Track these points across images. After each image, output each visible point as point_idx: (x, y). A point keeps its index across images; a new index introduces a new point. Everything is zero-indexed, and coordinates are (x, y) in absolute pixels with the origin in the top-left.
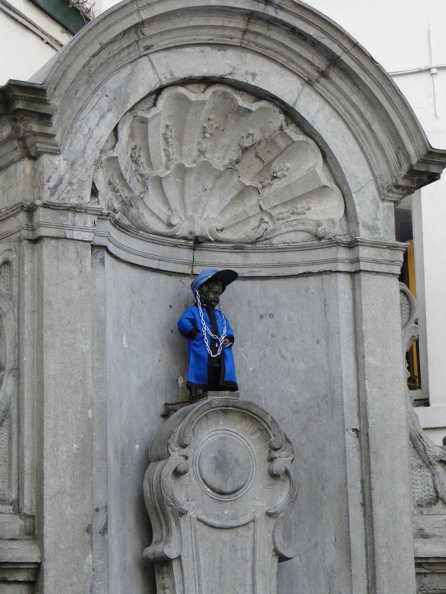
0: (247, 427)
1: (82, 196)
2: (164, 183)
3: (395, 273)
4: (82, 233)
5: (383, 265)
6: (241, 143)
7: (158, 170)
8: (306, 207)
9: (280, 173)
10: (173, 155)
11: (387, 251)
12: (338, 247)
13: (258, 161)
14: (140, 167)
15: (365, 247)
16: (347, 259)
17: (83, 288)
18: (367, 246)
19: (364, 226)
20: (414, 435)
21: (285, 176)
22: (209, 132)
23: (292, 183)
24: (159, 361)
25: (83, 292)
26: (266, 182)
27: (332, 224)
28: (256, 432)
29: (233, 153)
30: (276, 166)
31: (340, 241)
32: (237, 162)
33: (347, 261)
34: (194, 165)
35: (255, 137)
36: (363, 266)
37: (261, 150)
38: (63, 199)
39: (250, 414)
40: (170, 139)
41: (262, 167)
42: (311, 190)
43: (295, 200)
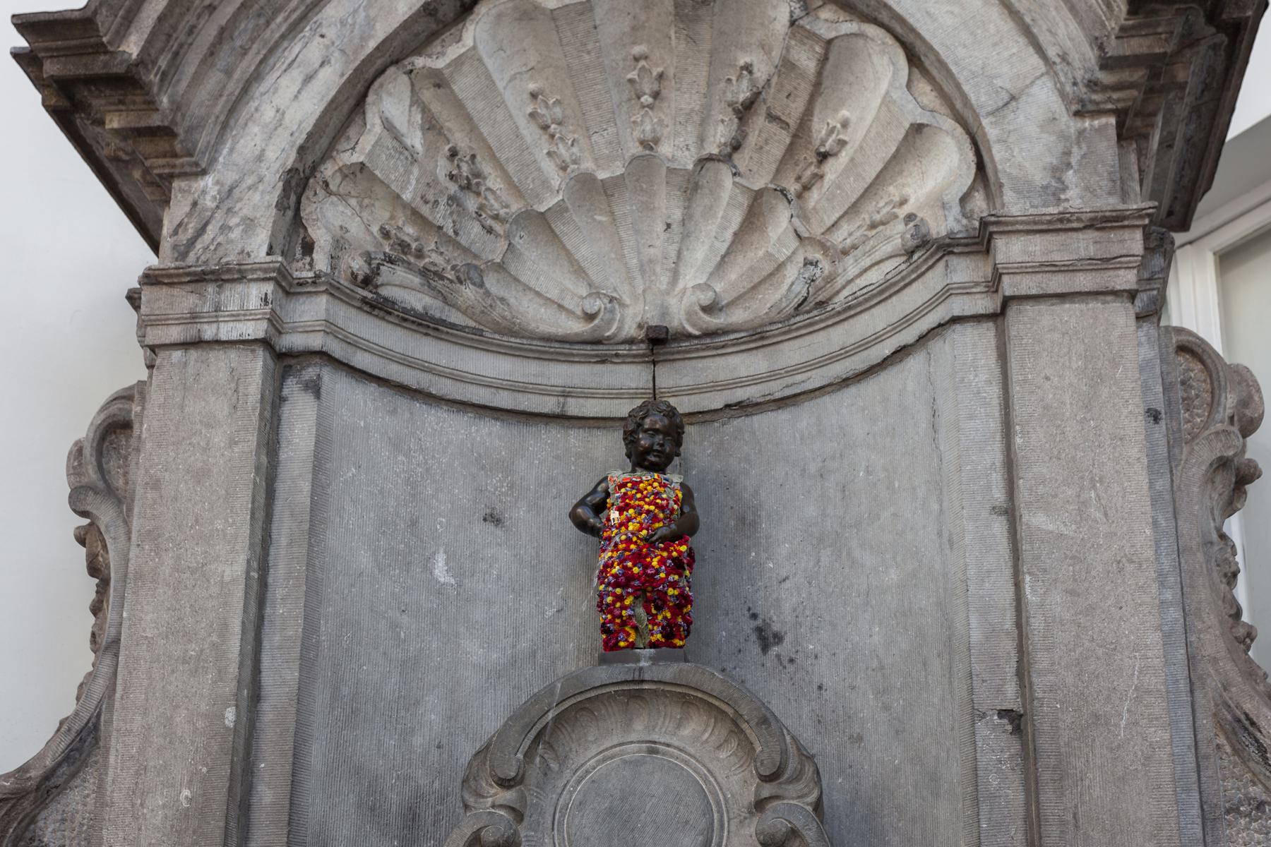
0: (705, 731)
1: (248, 249)
2: (559, 228)
3: (1118, 288)
4: (239, 325)
5: (1079, 274)
6: (729, 97)
7: (541, 202)
8: (897, 199)
9: (830, 141)
10: (575, 162)
11: (1086, 236)
12: (946, 258)
13: (774, 128)
14: (486, 198)
15: (1014, 238)
16: (977, 284)
17: (236, 443)
18: (1018, 232)
19: (1017, 191)
20: (1229, 717)
21: (842, 143)
22: (647, 91)
23: (856, 152)
24: (558, 611)
25: (236, 450)
26: (808, 173)
27: (941, 212)
28: (726, 741)
29: (721, 128)
30: (819, 129)
31: (948, 241)
32: (736, 147)
33: (978, 290)
34: (619, 171)
35: (757, 74)
36: (1009, 286)
37: (772, 99)
38: (206, 262)
39: (700, 695)
40: (553, 126)
41: (788, 140)
42: (894, 149)
43: (870, 190)
